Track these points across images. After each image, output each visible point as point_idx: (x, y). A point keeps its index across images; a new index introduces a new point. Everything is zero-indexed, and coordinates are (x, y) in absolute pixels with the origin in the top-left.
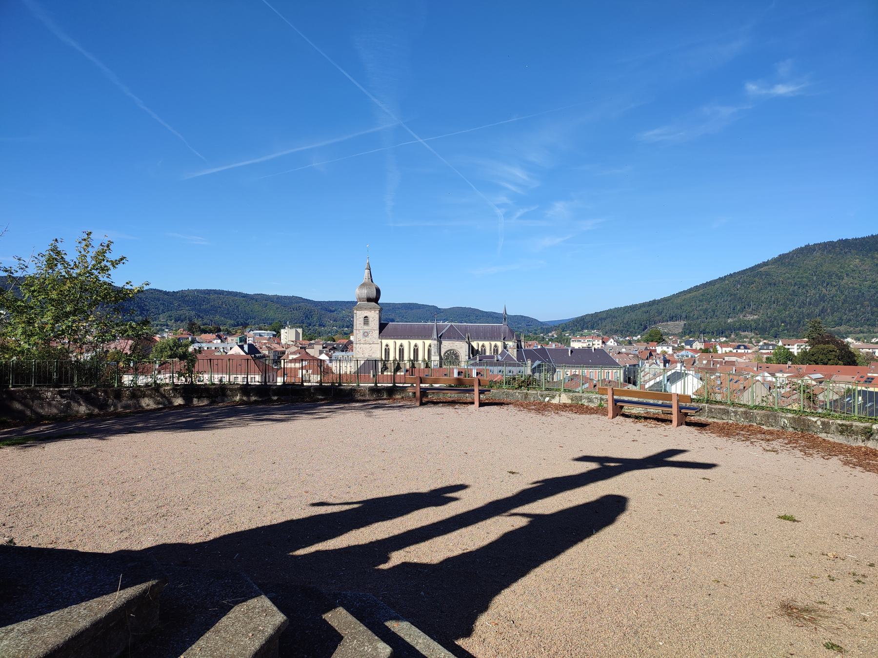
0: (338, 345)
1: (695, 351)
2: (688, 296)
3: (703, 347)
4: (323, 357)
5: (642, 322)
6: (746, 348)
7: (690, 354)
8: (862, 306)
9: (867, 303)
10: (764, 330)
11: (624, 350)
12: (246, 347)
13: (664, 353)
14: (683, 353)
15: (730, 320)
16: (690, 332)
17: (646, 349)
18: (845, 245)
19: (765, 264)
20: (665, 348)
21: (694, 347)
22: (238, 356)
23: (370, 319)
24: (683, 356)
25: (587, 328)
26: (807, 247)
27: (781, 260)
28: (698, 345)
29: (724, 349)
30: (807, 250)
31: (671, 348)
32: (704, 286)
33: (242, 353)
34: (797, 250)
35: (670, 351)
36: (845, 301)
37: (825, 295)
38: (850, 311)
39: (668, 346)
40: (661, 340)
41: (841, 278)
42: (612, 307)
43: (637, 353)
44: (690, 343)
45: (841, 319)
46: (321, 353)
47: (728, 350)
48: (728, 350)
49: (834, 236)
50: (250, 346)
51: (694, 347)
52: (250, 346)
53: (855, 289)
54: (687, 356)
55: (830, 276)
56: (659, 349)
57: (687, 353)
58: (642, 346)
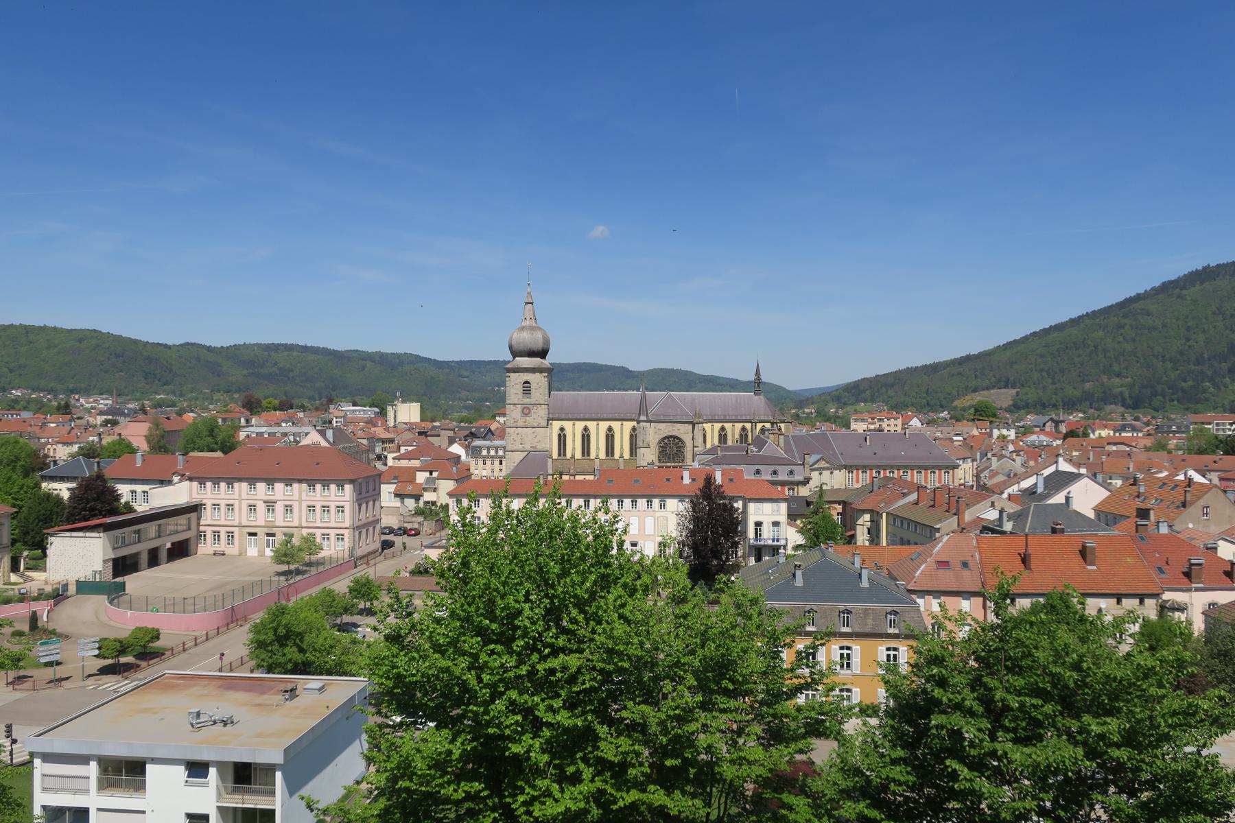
0: (478, 428)
4: (457, 449)
6: (1134, 429)
12: (329, 434)
15: (1087, 385)
19: (1139, 298)
20: (1004, 432)
22: (315, 447)
23: (534, 386)
25: (865, 401)
26: (1206, 269)
32: (1046, 332)
33: (324, 444)
35: (1012, 434)
39: (1008, 426)
42: (903, 367)
46: (451, 441)
50: (337, 431)
52: (337, 431)
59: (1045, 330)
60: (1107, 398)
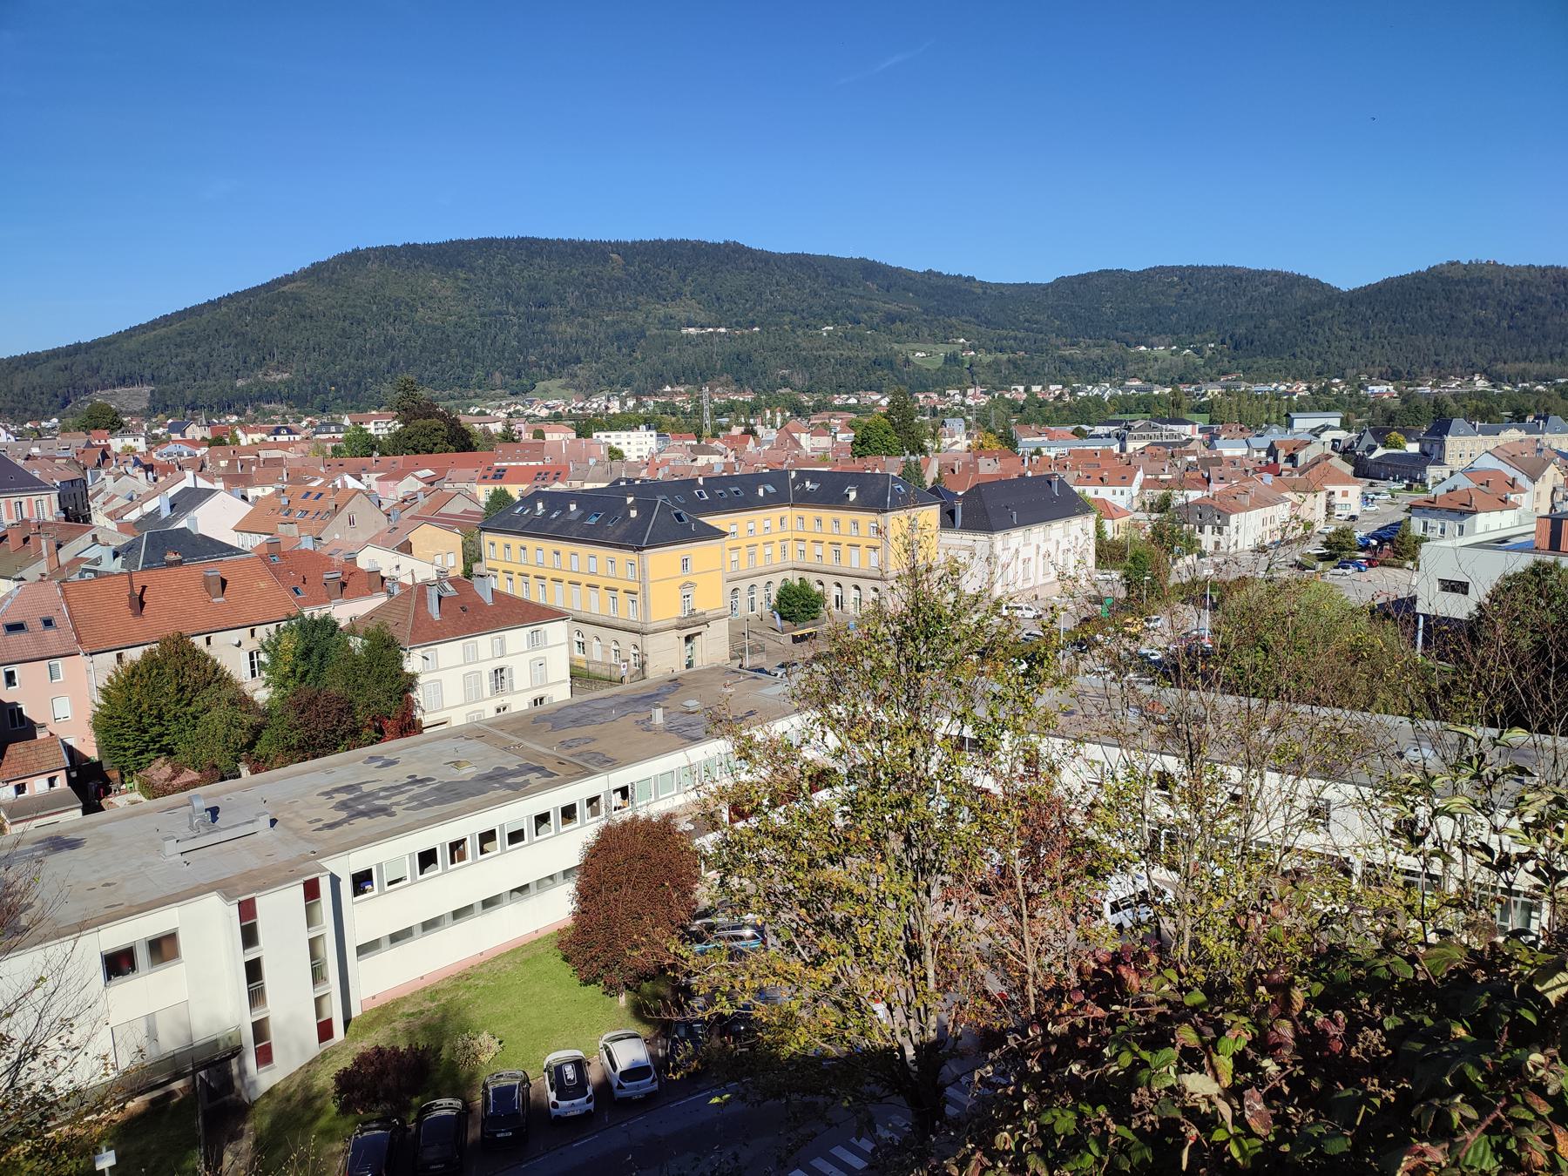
1: (194, 443)
2: (162, 331)
3: (208, 434)
5: (67, 386)
7: (185, 450)
8: (449, 356)
9: (454, 351)
10: (309, 399)
11: (35, 450)
13: (130, 451)
14: (171, 448)
16: (172, 405)
17: (89, 444)
18: (413, 252)
19: (289, 279)
20: (129, 441)
21: (189, 436)
24: (169, 455)
27: (316, 272)
28: (195, 432)
29: (250, 436)
30: (356, 259)
31: (142, 440)
34: (340, 256)
35: (141, 445)
36: (423, 349)
37: (392, 339)
38: (433, 364)
40: (115, 425)
41: (413, 309)
43: (69, 454)
44: (179, 428)
45: (420, 377)
47: (257, 437)
48: (257, 437)
49: (397, 237)
51: (189, 436)
53: (435, 328)
54: (181, 455)
55: (397, 306)
56: (116, 444)
57: (175, 449)
58: (79, 440)
59: (178, 313)
60: (270, 395)
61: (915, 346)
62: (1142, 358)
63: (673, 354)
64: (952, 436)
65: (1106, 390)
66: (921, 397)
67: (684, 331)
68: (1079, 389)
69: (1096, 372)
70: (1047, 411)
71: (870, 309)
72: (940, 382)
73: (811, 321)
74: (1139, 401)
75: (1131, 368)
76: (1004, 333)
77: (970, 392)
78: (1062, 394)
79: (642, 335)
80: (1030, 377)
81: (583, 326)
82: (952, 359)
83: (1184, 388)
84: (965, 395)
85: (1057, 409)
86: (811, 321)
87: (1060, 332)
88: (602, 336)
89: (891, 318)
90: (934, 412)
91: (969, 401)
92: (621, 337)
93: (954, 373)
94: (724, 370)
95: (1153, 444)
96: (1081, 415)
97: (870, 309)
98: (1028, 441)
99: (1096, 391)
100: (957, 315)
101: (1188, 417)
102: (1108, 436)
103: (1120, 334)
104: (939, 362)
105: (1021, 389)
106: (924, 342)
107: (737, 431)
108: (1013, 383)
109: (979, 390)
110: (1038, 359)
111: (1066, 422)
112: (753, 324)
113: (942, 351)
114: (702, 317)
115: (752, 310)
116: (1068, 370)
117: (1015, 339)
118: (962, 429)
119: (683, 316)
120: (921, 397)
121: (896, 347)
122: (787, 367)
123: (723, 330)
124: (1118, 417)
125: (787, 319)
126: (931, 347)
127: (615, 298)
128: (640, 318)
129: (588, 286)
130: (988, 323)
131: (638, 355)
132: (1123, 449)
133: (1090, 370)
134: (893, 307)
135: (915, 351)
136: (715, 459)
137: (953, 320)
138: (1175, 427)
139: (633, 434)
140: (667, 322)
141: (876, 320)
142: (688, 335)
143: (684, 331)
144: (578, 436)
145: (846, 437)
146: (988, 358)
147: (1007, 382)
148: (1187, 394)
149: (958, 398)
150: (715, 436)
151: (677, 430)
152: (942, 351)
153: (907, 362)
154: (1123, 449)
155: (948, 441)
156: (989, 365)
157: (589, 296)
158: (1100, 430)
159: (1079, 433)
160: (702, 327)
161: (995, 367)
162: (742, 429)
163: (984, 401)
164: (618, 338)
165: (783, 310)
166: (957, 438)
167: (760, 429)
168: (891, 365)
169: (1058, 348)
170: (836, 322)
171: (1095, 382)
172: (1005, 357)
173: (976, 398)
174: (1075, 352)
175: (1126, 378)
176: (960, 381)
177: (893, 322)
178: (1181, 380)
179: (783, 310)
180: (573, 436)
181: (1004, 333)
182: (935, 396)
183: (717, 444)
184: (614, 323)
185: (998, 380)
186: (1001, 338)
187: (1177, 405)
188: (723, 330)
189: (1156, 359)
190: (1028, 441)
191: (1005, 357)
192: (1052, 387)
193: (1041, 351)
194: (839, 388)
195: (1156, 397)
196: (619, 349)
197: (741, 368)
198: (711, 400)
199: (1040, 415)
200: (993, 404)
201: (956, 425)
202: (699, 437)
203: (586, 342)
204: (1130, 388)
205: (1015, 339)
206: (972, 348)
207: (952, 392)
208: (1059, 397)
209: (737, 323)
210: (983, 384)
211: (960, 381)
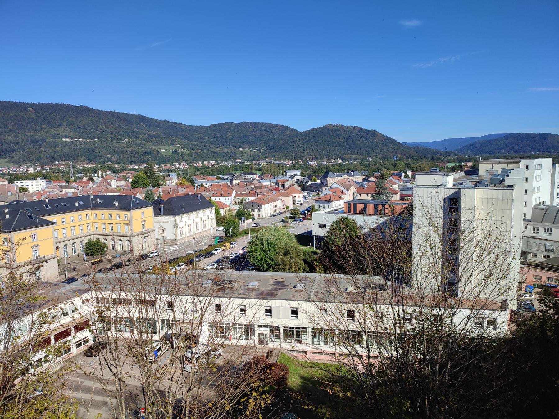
61: (161, 147)
62: (241, 152)
63: (59, 148)
64: (172, 180)
65: (229, 163)
66: (163, 165)
67: (64, 140)
68: (220, 163)
69: (226, 157)
70: (209, 171)
71: (143, 133)
72: (170, 160)
73: (119, 137)
74: (240, 167)
75: (238, 155)
76: (193, 143)
77: (182, 164)
78: (214, 164)
79: (45, 141)
80: (203, 158)
81: (16, 137)
82: (175, 152)
83: (254, 162)
84: (180, 165)
85: (212, 170)
86: (119, 137)
87: (213, 143)
88: (25, 141)
89: (151, 137)
90: (168, 171)
91: (181, 167)
92: (34, 142)
93: (175, 157)
94: (82, 155)
95: (241, 182)
96: (219, 172)
97: (143, 133)
98: (199, 181)
99: (226, 163)
100: (176, 136)
101: (255, 172)
102: (227, 179)
103: (233, 144)
104: (170, 153)
105: (200, 163)
106: (164, 145)
107: (85, 179)
108: (197, 160)
109: (185, 163)
110: (206, 152)
111: (215, 174)
112: (94, 138)
113: (171, 149)
114: (72, 134)
115: (93, 132)
116: (216, 156)
117: (197, 145)
118: (176, 177)
119: (63, 134)
120: (163, 165)
121: (153, 147)
122: (110, 154)
123: (81, 140)
124: (232, 172)
125: (109, 136)
126: (167, 147)
127: (31, 126)
128: (43, 134)
129: (18, 120)
130: (187, 139)
131: (43, 149)
132: (232, 183)
133: (224, 156)
134: (152, 133)
135: (161, 149)
136: (73, 190)
137: (175, 138)
138: (249, 176)
139: (34, 182)
140: (56, 136)
141: (145, 137)
142: (65, 142)
143: (64, 140)
144: (9, 183)
145: (130, 181)
146: (188, 152)
147: (195, 160)
148: (256, 164)
149: (177, 166)
150: (75, 181)
151: (58, 179)
152: (171, 149)
153: (158, 153)
154: (232, 183)
155: (171, 182)
156: (188, 154)
157: (19, 125)
158: (226, 177)
159: (218, 178)
160: (72, 138)
161: (190, 155)
162: (87, 178)
163: (187, 167)
164: (33, 142)
165: (107, 132)
166: (174, 180)
167: (95, 178)
168: (152, 154)
169: (213, 148)
170: (129, 138)
171: (226, 160)
172: (194, 151)
173: (184, 166)
174: (219, 150)
175: (236, 159)
176: (178, 160)
177: (152, 138)
178: (254, 160)
179: (107, 132)
180: (6, 182)
181: (193, 143)
182: (168, 165)
183: (74, 185)
184: (31, 136)
185: (192, 159)
186: (192, 145)
187: (251, 168)
188: (81, 140)
189: (245, 153)
190: (199, 181)
191: (194, 151)
192: (211, 162)
193: (207, 149)
194: (131, 162)
195: (245, 165)
196: (34, 146)
197: (90, 154)
198: (74, 167)
199: (205, 172)
200: (190, 169)
201: (174, 176)
202: (67, 181)
203: (17, 144)
204: (238, 162)
205: (197, 145)
206: (182, 148)
207: (175, 164)
208: (213, 166)
209: (88, 137)
210: (186, 161)
211: (178, 160)
